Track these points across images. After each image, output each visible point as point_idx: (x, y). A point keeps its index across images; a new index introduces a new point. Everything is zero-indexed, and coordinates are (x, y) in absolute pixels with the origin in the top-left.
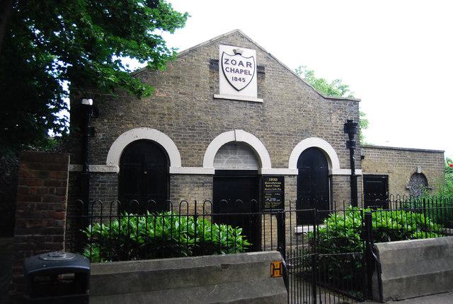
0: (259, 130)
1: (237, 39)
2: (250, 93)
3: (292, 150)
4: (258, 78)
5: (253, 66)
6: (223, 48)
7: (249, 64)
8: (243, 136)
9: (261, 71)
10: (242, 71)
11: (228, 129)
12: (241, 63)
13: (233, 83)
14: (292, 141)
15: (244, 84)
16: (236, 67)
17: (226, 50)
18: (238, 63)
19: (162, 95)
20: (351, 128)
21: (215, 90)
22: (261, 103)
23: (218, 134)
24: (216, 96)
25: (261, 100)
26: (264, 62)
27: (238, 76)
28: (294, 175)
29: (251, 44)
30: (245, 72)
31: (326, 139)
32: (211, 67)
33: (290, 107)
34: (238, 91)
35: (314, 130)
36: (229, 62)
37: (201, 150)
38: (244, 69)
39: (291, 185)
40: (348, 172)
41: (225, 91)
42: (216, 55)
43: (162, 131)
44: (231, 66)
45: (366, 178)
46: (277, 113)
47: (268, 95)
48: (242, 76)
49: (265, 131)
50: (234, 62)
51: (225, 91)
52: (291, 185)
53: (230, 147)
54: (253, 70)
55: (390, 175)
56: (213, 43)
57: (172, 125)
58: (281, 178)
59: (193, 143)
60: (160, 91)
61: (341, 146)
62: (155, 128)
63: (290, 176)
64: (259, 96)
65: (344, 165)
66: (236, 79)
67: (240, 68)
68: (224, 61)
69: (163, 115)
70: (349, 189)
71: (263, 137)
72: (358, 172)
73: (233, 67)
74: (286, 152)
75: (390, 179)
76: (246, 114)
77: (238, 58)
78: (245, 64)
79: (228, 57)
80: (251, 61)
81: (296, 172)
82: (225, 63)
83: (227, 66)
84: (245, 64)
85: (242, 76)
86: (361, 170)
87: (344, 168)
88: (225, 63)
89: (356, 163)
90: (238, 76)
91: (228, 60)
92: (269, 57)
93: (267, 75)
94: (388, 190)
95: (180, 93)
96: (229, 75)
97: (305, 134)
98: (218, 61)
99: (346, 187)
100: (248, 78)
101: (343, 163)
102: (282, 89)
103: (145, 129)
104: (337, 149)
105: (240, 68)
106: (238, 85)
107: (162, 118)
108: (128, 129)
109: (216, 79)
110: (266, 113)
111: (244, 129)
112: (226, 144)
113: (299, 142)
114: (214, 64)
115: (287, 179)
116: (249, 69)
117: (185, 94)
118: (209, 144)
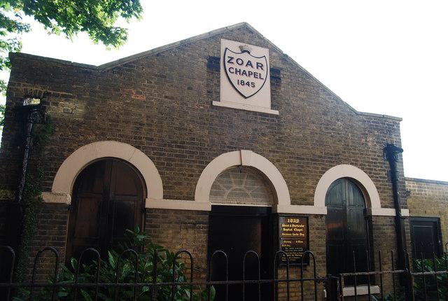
0: (274, 152)
1: (245, 34)
2: (261, 102)
3: (318, 180)
4: (272, 84)
5: (265, 68)
6: (225, 43)
7: (259, 66)
8: (252, 159)
9: (275, 75)
10: (250, 73)
11: (232, 149)
12: (249, 64)
13: (240, 88)
14: (318, 168)
15: (253, 91)
16: (243, 68)
17: (230, 47)
18: (245, 64)
19: (140, 97)
20: (392, 153)
21: (215, 96)
22: (277, 116)
23: (217, 155)
24: (215, 103)
25: (276, 112)
26: (279, 65)
27: (245, 79)
28: (322, 215)
29: (262, 42)
30: (255, 75)
31: (362, 167)
32: (209, 66)
33: (314, 123)
34: (246, 98)
35: (347, 154)
36: (234, 61)
38: (253, 70)
39: (317, 229)
40: (391, 212)
41: (228, 98)
42: (216, 52)
43: (138, 147)
44: (236, 66)
46: (297, 130)
47: (284, 106)
48: (251, 79)
49: (282, 153)
50: (240, 62)
51: (228, 98)
52: (317, 229)
53: (251, 177)
54: (265, 73)
55: (442, 218)
56: (214, 38)
57: (152, 139)
58: (304, 218)
59: (182, 165)
60: (138, 93)
61: (381, 177)
62: (128, 142)
63: (316, 216)
64: (273, 107)
65: (386, 203)
66: (242, 83)
67: (248, 69)
68: (227, 59)
69: (141, 125)
70: (393, 235)
71: (278, 161)
72: (405, 212)
73: (239, 67)
74: (310, 183)
75: (442, 223)
76: (256, 130)
77: (246, 58)
78: (255, 65)
79: (232, 55)
80: (262, 61)
81: (324, 211)
82: (229, 62)
83: (231, 65)
84: (255, 65)
85: (251, 79)
86: (408, 210)
87: (386, 207)
88: (229, 62)
89: (401, 200)
90: (245, 79)
91: (232, 58)
92: (285, 58)
93: (283, 81)
94: (441, 238)
95: (166, 97)
96: (234, 78)
97: (336, 160)
98: (219, 59)
99: (390, 231)
100: (258, 83)
101: (385, 200)
102: (303, 100)
103: (113, 143)
104: (375, 180)
105: (248, 69)
106: (246, 90)
107: (138, 129)
108: (88, 142)
109: (215, 82)
110: (283, 130)
111: (253, 150)
112: (251, 167)
113: (327, 169)
114: (214, 64)
115: (312, 221)
116: (259, 71)
117: (172, 98)
118: (324, 172)
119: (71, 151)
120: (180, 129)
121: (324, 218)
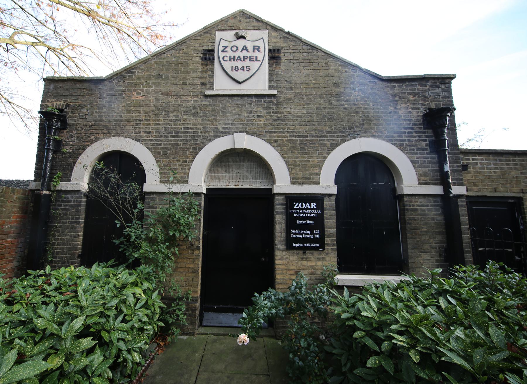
0: (271, 132)
3: (325, 158)
4: (270, 65)
5: (262, 50)
6: (219, 35)
7: (256, 48)
10: (245, 58)
11: (224, 133)
13: (234, 74)
14: (325, 145)
16: (239, 54)
19: (140, 98)
21: (208, 86)
22: (274, 96)
23: (209, 141)
25: (274, 92)
26: (280, 44)
27: (239, 64)
30: (251, 59)
33: (321, 96)
36: (228, 49)
37: (185, 161)
38: (248, 54)
43: (138, 140)
44: (230, 53)
45: (471, 201)
46: (299, 108)
57: (150, 133)
59: (176, 153)
60: (138, 94)
62: (130, 137)
64: (271, 87)
65: (427, 179)
66: (237, 69)
68: (221, 49)
69: (140, 120)
71: (276, 141)
72: (457, 190)
76: (251, 112)
77: (241, 43)
78: (250, 48)
79: (226, 44)
80: (260, 44)
82: (223, 51)
84: (250, 48)
85: (247, 63)
88: (223, 51)
90: (239, 64)
91: (226, 47)
93: (284, 60)
95: (162, 94)
96: (227, 65)
101: (425, 175)
103: (117, 138)
104: (409, 153)
105: (245, 53)
106: (240, 76)
107: (137, 124)
108: (97, 140)
109: (209, 72)
111: (247, 133)
113: (337, 145)
116: (256, 53)
117: (168, 94)
119: (84, 149)
120: (174, 121)
121: (333, 198)
